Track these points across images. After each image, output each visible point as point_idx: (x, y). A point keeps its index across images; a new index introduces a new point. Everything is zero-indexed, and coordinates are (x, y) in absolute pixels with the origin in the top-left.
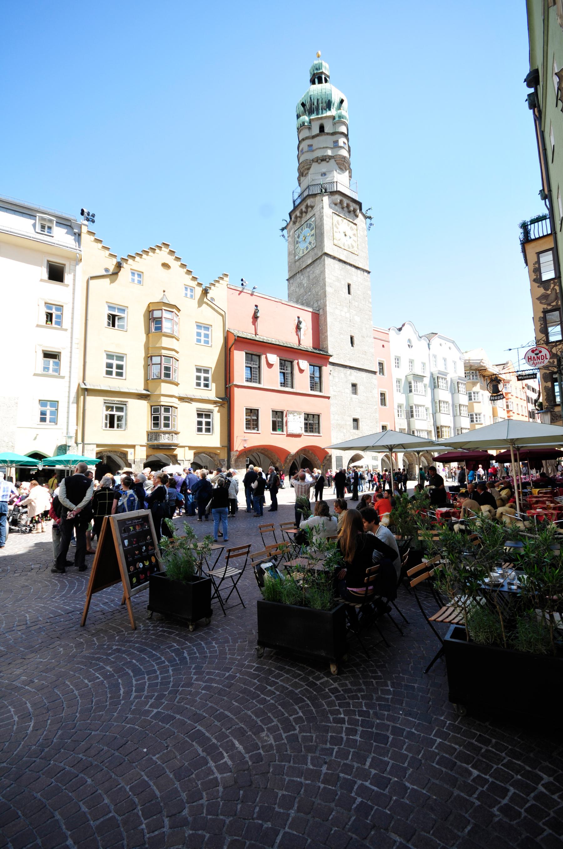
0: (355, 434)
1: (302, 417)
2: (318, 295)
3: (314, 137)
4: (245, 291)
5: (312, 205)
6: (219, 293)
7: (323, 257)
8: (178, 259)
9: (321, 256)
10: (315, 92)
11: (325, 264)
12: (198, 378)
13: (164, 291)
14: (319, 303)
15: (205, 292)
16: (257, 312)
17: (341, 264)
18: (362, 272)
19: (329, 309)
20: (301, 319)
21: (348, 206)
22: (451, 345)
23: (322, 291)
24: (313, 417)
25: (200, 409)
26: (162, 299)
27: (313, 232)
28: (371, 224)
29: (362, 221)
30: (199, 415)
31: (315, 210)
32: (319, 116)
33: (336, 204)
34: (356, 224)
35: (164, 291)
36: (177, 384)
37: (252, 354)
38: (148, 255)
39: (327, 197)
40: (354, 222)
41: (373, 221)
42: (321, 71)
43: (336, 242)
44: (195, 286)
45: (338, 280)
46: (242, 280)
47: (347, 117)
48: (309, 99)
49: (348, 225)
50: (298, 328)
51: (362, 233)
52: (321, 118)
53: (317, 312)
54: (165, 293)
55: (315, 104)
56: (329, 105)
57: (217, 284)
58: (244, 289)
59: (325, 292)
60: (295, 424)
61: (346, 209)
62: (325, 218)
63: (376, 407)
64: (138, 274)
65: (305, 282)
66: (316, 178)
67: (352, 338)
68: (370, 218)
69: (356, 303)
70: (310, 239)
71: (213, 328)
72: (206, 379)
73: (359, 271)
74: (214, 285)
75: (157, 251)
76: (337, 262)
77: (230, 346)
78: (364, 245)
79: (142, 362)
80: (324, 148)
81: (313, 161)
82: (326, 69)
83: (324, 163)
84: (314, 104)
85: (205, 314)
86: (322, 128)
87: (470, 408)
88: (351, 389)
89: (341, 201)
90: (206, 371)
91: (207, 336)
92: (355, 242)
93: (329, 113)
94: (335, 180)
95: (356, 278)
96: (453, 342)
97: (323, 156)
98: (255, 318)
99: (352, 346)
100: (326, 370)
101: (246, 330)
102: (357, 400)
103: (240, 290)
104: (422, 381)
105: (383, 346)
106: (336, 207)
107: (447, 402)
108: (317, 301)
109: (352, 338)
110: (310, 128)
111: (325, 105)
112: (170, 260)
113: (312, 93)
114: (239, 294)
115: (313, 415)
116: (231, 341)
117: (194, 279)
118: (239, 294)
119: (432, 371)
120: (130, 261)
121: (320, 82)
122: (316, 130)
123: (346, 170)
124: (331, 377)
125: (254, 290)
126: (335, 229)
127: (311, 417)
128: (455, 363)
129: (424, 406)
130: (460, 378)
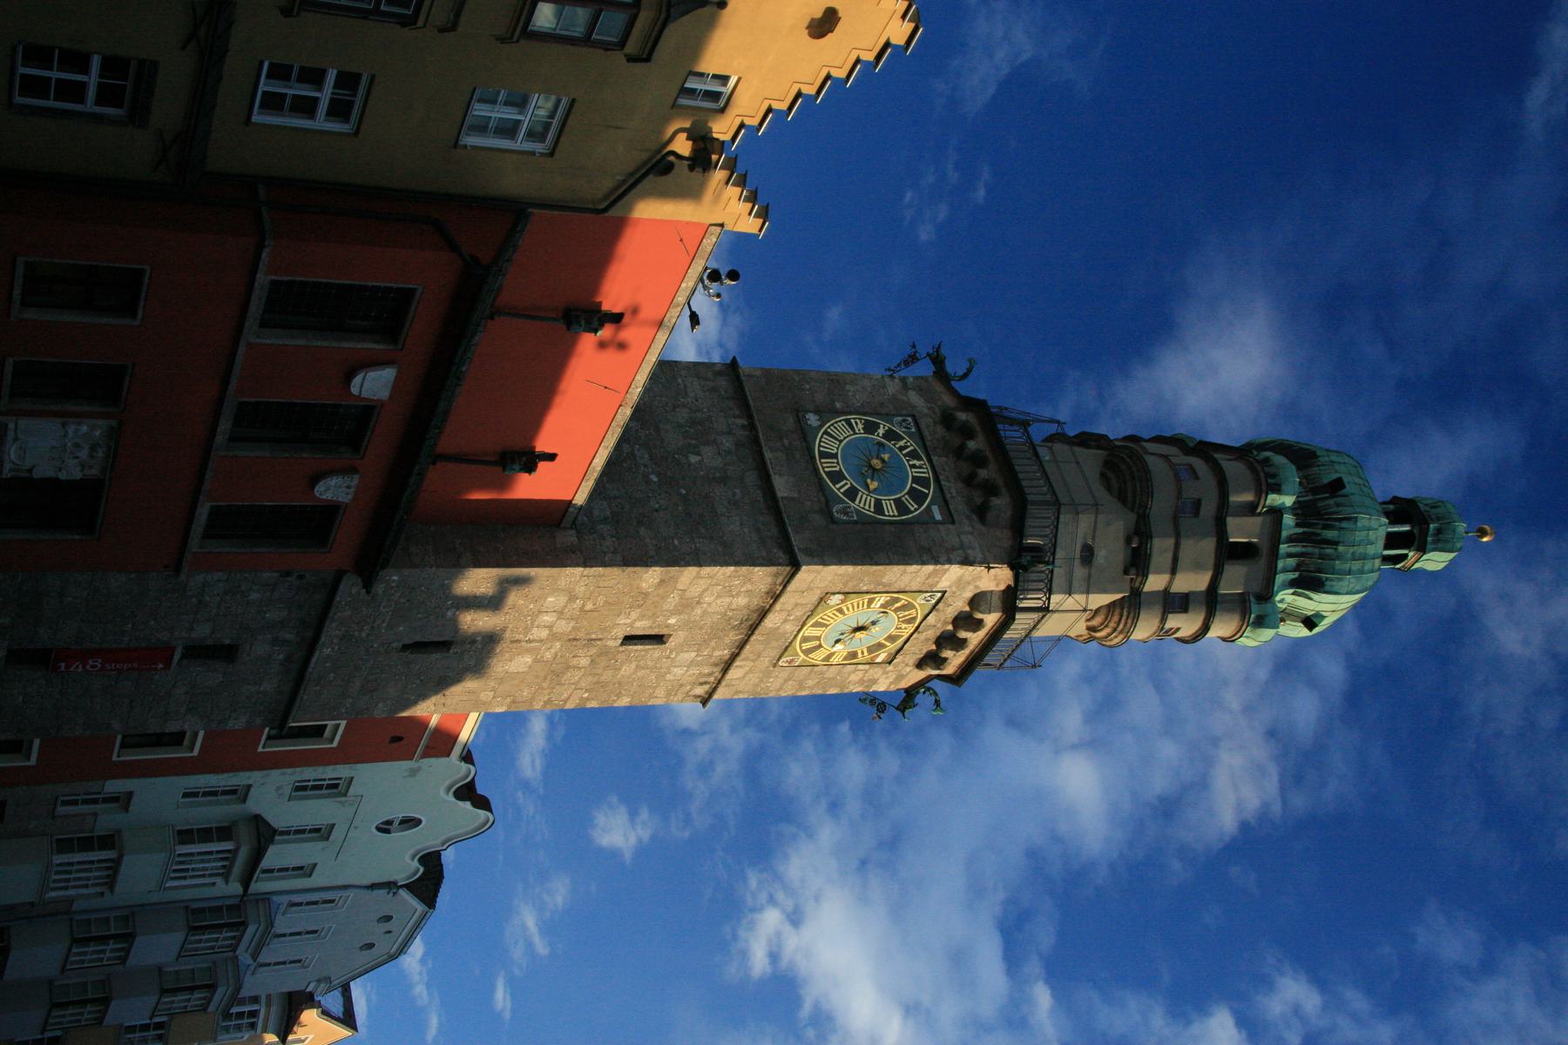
14: (604, 528)
27: (890, 510)
29: (900, 677)
45: (686, 605)
49: (891, 638)
51: (853, 677)
53: (568, 520)
59: (644, 561)
65: (707, 458)
69: (584, 662)
73: (710, 671)
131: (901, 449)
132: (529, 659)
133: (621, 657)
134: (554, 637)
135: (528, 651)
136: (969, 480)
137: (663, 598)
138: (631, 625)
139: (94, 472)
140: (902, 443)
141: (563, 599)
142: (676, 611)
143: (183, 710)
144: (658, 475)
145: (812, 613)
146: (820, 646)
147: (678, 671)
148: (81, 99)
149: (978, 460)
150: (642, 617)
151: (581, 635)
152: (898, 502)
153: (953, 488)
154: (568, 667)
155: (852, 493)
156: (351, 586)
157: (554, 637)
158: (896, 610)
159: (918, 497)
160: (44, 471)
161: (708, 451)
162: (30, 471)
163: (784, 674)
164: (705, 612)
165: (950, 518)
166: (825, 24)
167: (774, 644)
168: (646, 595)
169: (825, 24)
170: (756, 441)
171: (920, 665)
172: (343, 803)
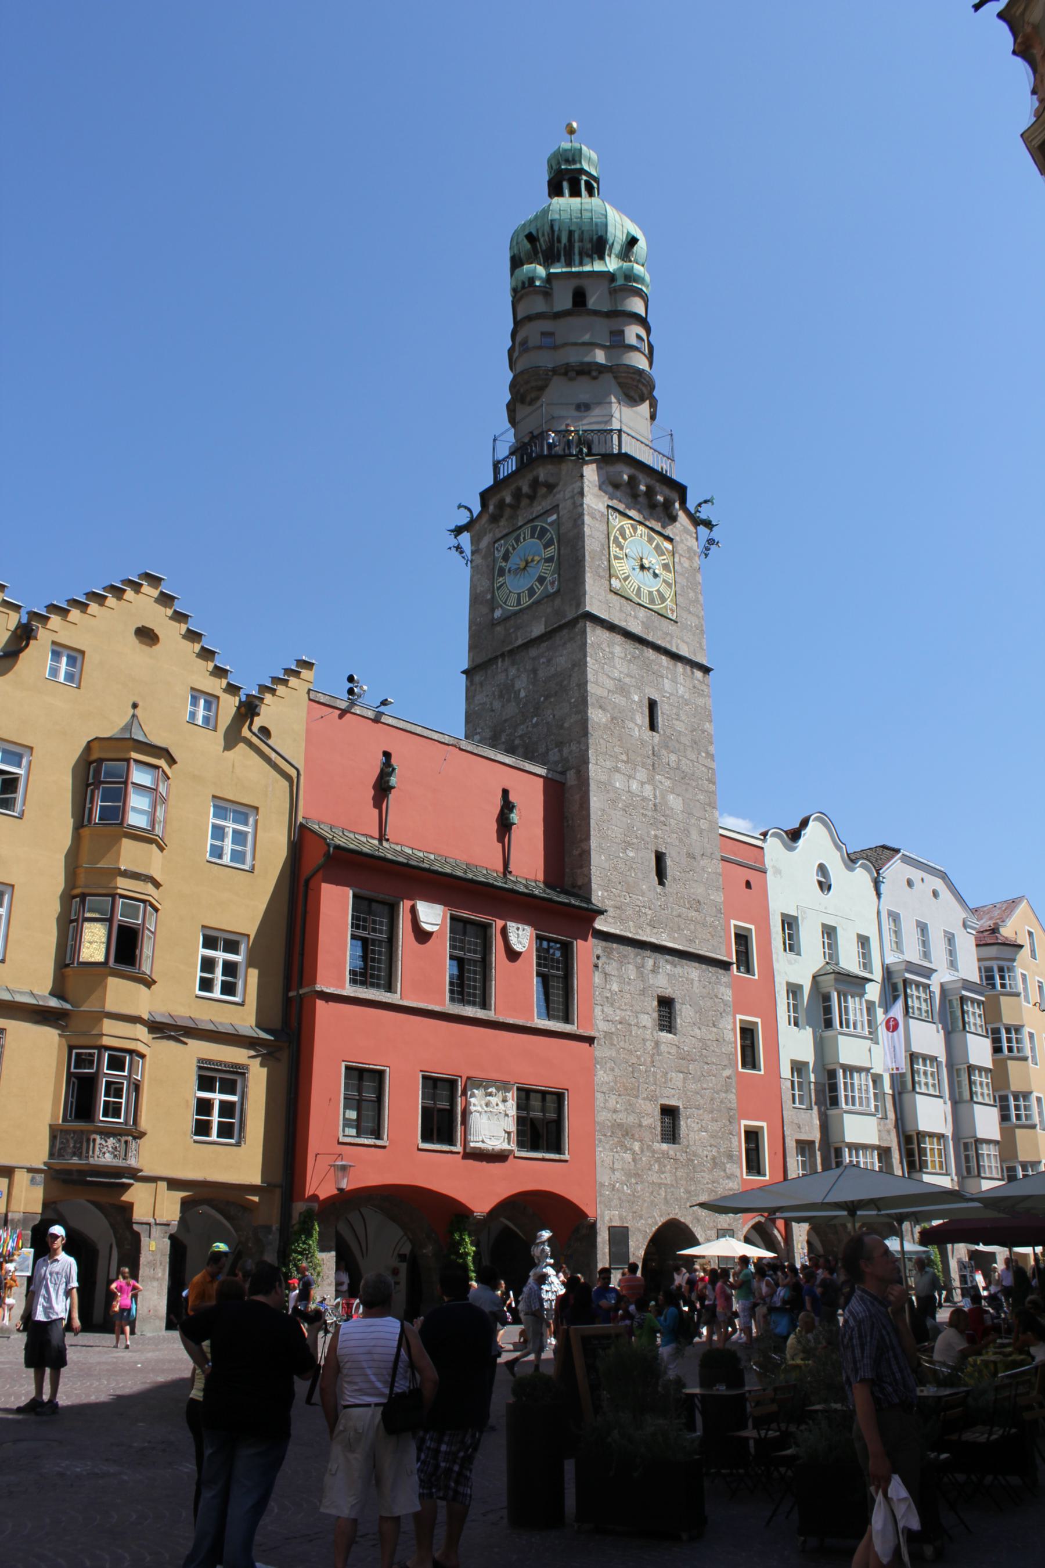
0: (665, 1155)
1: (512, 1097)
2: (561, 727)
4: (357, 710)
5: (551, 480)
6: (285, 715)
7: (580, 625)
8: (180, 617)
9: (575, 621)
10: (565, 216)
11: (585, 644)
12: (208, 965)
13: (135, 706)
14: (566, 751)
15: (249, 709)
16: (390, 774)
17: (630, 646)
18: (688, 668)
19: (595, 771)
20: (512, 798)
21: (650, 493)
22: (938, 884)
23: (575, 718)
24: (544, 1100)
25: (210, 1061)
26: (128, 727)
27: (552, 551)
28: (711, 542)
29: (686, 530)
30: (205, 1083)
31: (560, 496)
32: (574, 270)
33: (616, 486)
35: (135, 706)
36: (149, 983)
37: (370, 901)
38: (102, 605)
39: (594, 466)
40: (669, 531)
41: (715, 534)
42: (578, 166)
44: (218, 692)
45: (622, 689)
46: (351, 679)
47: (647, 278)
48: (547, 228)
49: (650, 540)
50: (504, 826)
53: (558, 777)
54: (138, 712)
55: (564, 240)
56: (599, 247)
57: (281, 689)
58: (353, 704)
59: (584, 722)
60: (491, 1122)
61: (642, 499)
62: (587, 519)
63: (727, 1072)
64: (69, 657)
67: (660, 858)
68: (708, 524)
69: (673, 757)
71: (260, 817)
72: (230, 968)
74: (273, 691)
75: (129, 594)
76: (618, 638)
77: (307, 870)
78: (692, 595)
79: (56, 908)
80: (584, 344)
81: (555, 371)
82: (590, 162)
83: (583, 382)
84: (559, 241)
85: (246, 773)
86: (580, 298)
87: (999, 1075)
88: (656, 1015)
90: (231, 946)
91: (239, 837)
93: (598, 267)
94: (616, 425)
95: (674, 685)
96: (943, 876)
97: (582, 364)
98: (382, 789)
99: (661, 883)
100: (585, 949)
101: (353, 826)
102: (673, 1051)
103: (343, 705)
104: (861, 995)
105: (748, 885)
106: (618, 494)
107: (934, 1059)
108: (560, 745)
109: (660, 858)
110: (546, 292)
111: (589, 246)
112: (158, 618)
113: (557, 217)
114: (341, 717)
115: (544, 1094)
116: (314, 858)
117: (219, 672)
118: (341, 717)
119: (887, 961)
120: (55, 620)
121: (575, 193)
122: (564, 301)
123: (642, 400)
124: (598, 978)
125: (382, 709)
126: (614, 550)
127: (535, 1102)
128: (950, 939)
129: (867, 1070)
130: (967, 985)
131: (514, 549)
133: (669, 731)
134: (651, 781)
135: (663, 797)
136: (532, 498)
138: (640, 727)
140: (510, 549)
141: (617, 776)
143: (714, 1029)
144: (532, 718)
146: (658, 591)
147: (681, 690)
149: (518, 495)
150: (633, 720)
151: (649, 762)
153: (538, 509)
157: (651, 781)
159: (544, 531)
161: (518, 684)
162: (509, 1133)
163: (685, 615)
164: (628, 675)
165: (555, 508)
166: (146, 635)
167: (656, 623)
169: (146, 635)
170: (511, 652)
172: (803, 919)
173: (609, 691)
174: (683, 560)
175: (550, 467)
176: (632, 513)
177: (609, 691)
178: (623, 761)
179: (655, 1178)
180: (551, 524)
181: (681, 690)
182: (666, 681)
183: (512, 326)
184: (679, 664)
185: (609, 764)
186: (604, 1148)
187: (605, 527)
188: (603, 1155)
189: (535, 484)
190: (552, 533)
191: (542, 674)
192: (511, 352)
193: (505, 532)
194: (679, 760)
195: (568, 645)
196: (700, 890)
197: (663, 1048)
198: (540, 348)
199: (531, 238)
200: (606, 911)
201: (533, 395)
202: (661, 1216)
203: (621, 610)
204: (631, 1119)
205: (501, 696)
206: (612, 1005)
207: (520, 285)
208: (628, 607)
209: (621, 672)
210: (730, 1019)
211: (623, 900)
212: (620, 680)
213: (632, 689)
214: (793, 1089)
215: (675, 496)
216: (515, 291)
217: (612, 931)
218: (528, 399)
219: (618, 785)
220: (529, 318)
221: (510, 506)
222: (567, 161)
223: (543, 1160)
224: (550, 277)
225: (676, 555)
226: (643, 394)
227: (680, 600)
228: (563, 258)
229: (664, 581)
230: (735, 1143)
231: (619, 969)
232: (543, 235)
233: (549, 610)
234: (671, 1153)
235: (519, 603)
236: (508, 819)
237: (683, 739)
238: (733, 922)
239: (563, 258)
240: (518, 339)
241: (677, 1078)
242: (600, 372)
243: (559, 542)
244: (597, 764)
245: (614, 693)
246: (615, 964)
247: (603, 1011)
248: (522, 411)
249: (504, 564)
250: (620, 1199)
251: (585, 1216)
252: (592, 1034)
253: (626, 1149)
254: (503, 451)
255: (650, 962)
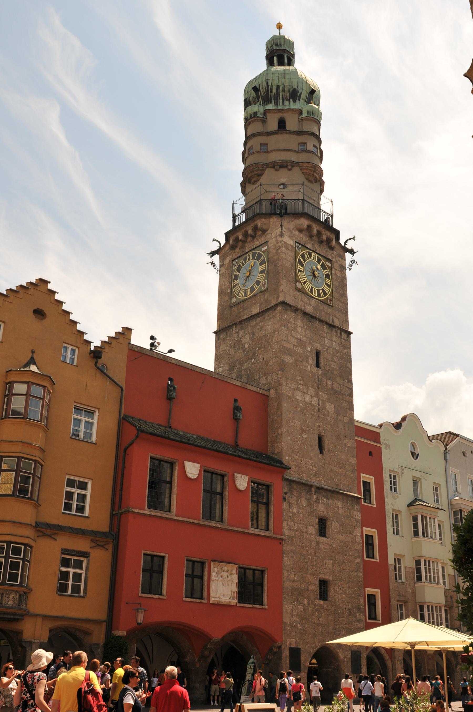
2: (267, 365)
3: (270, 134)
5: (264, 227)
9: (276, 306)
14: (269, 378)
18: (339, 331)
27: (264, 267)
28: (353, 261)
31: (270, 236)
33: (301, 231)
34: (330, 261)
41: (356, 257)
42: (283, 48)
43: (299, 285)
48: (265, 84)
52: (282, 111)
53: (265, 393)
55: (274, 91)
60: (223, 586)
61: (314, 238)
63: (358, 560)
66: (271, 190)
67: (320, 439)
68: (352, 252)
69: (329, 382)
70: (262, 278)
81: (267, 165)
84: (271, 91)
86: (282, 124)
88: (317, 527)
89: (309, 227)
92: (329, 286)
93: (293, 106)
99: (321, 452)
102: (327, 547)
108: (266, 374)
110: (264, 121)
111: (288, 94)
121: (281, 63)
122: (273, 125)
124: (285, 505)
131: (243, 265)
132: (328, 404)
134: (317, 395)
135: (324, 405)
136: (254, 237)
137: (298, 353)
138: (311, 365)
139: (234, 572)
140: (241, 264)
142: (304, 348)
143: (350, 536)
144: (252, 359)
145: (306, 294)
146: (323, 289)
148: (80, 575)
149: (246, 235)
150: (307, 361)
151: (316, 385)
152: (261, 264)
154: (332, 388)
155: (258, 283)
156: (292, 475)
157: (317, 395)
158: (305, 261)
159: (260, 256)
160: (234, 588)
162: (234, 592)
163: (337, 302)
164: (305, 336)
167: (321, 308)
168: (296, 361)
170: (240, 322)
171: (332, 249)
173: (294, 345)
174: (337, 272)
175: (264, 220)
176: (308, 246)
177: (294, 345)
178: (301, 384)
179: (315, 620)
180: (263, 252)
181: (334, 345)
182: (326, 340)
183: (244, 139)
184: (334, 330)
185: (293, 386)
186: (287, 602)
187: (294, 254)
188: (287, 607)
189: (255, 229)
190: (264, 257)
191: (257, 335)
192: (243, 153)
193: (238, 255)
194: (333, 384)
195: (272, 320)
196: (343, 456)
197: (322, 546)
198: (260, 152)
199: (256, 89)
200: (290, 468)
201: (255, 178)
202: (319, 642)
203: (302, 300)
204: (303, 586)
205: (235, 347)
206: (293, 521)
207: (249, 116)
208: (305, 299)
209: (301, 335)
210: (360, 530)
211: (300, 462)
212: (300, 340)
213: (307, 345)
214: (396, 571)
215: (333, 237)
216: (246, 119)
217: (294, 479)
218: (253, 181)
219: (298, 398)
220: (254, 135)
221: (242, 241)
222: (277, 45)
223: (253, 608)
224: (266, 112)
225: (333, 269)
226: (317, 179)
227: (335, 294)
228: (273, 101)
229: (326, 284)
230: (362, 602)
231: (297, 501)
232: (263, 88)
233: (262, 300)
234: (325, 606)
235: (245, 295)
236: (236, 416)
237: (335, 372)
238: (362, 475)
239: (273, 101)
240: (248, 147)
241: (329, 564)
242: (292, 167)
243: (268, 262)
244: (286, 386)
245: (297, 346)
246: (295, 498)
247: (288, 524)
248: (249, 188)
249: (237, 273)
250: (296, 632)
251: (274, 641)
252: (282, 537)
253: (300, 603)
254: (238, 210)
255: (315, 497)
